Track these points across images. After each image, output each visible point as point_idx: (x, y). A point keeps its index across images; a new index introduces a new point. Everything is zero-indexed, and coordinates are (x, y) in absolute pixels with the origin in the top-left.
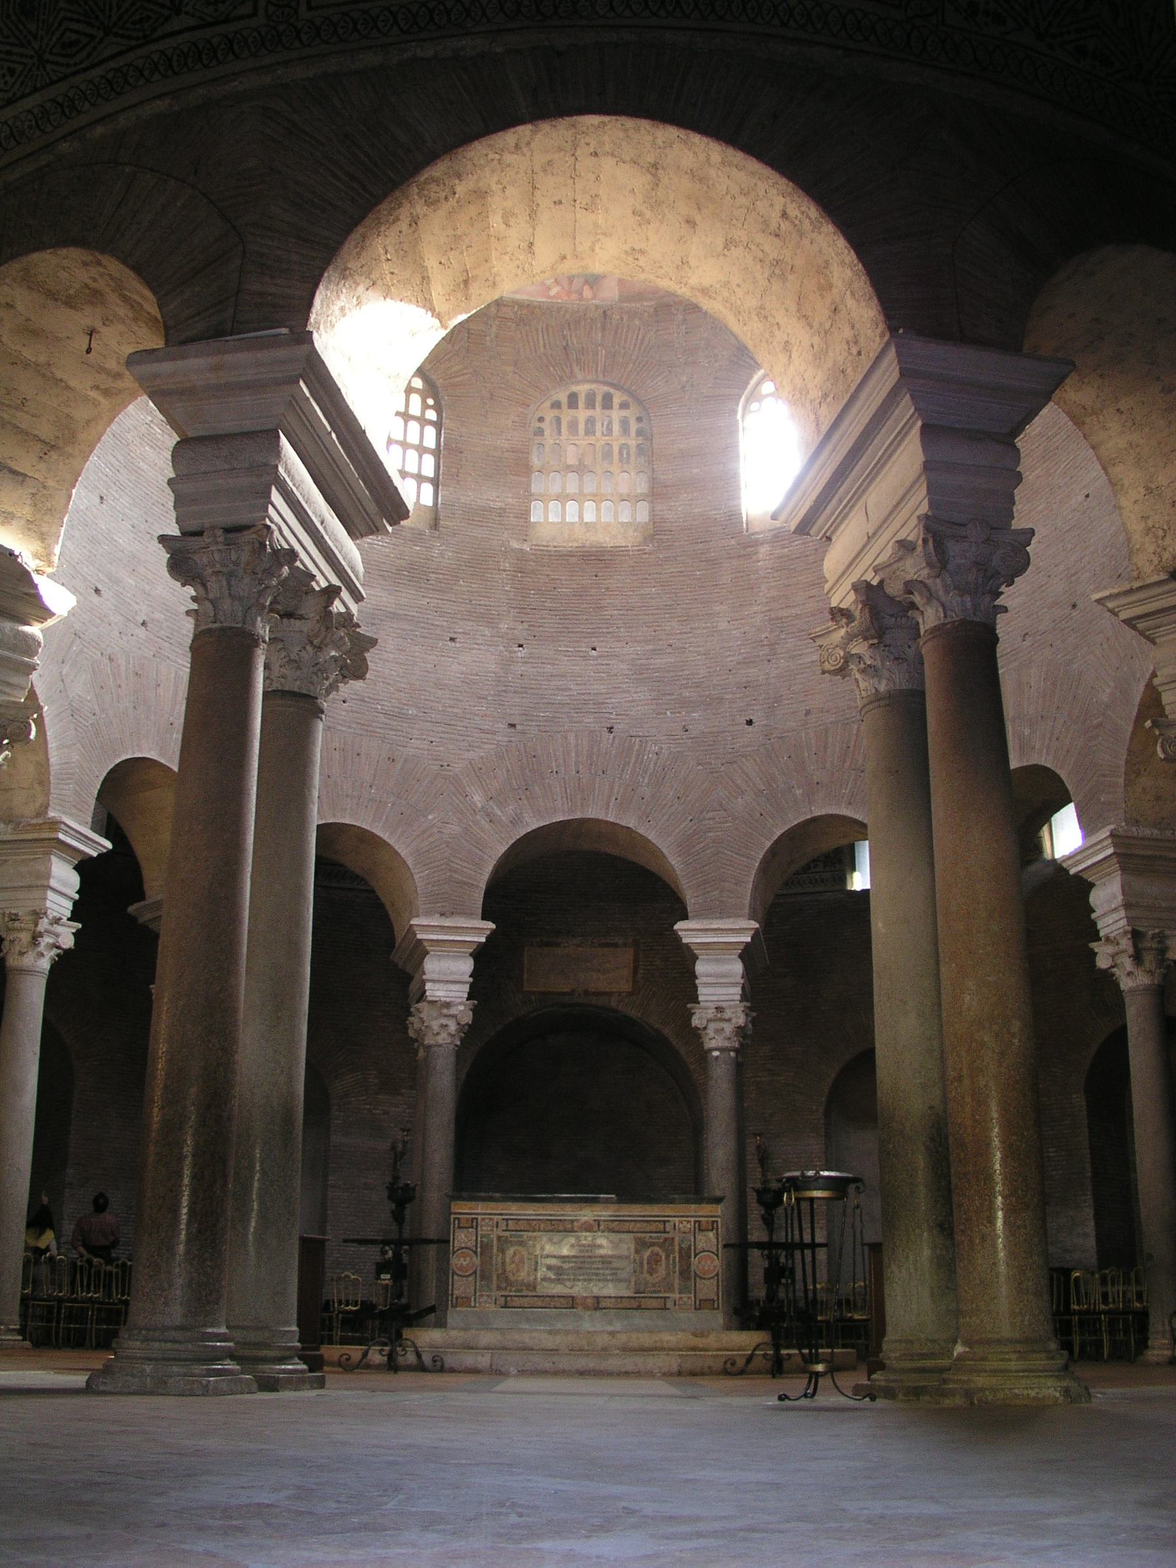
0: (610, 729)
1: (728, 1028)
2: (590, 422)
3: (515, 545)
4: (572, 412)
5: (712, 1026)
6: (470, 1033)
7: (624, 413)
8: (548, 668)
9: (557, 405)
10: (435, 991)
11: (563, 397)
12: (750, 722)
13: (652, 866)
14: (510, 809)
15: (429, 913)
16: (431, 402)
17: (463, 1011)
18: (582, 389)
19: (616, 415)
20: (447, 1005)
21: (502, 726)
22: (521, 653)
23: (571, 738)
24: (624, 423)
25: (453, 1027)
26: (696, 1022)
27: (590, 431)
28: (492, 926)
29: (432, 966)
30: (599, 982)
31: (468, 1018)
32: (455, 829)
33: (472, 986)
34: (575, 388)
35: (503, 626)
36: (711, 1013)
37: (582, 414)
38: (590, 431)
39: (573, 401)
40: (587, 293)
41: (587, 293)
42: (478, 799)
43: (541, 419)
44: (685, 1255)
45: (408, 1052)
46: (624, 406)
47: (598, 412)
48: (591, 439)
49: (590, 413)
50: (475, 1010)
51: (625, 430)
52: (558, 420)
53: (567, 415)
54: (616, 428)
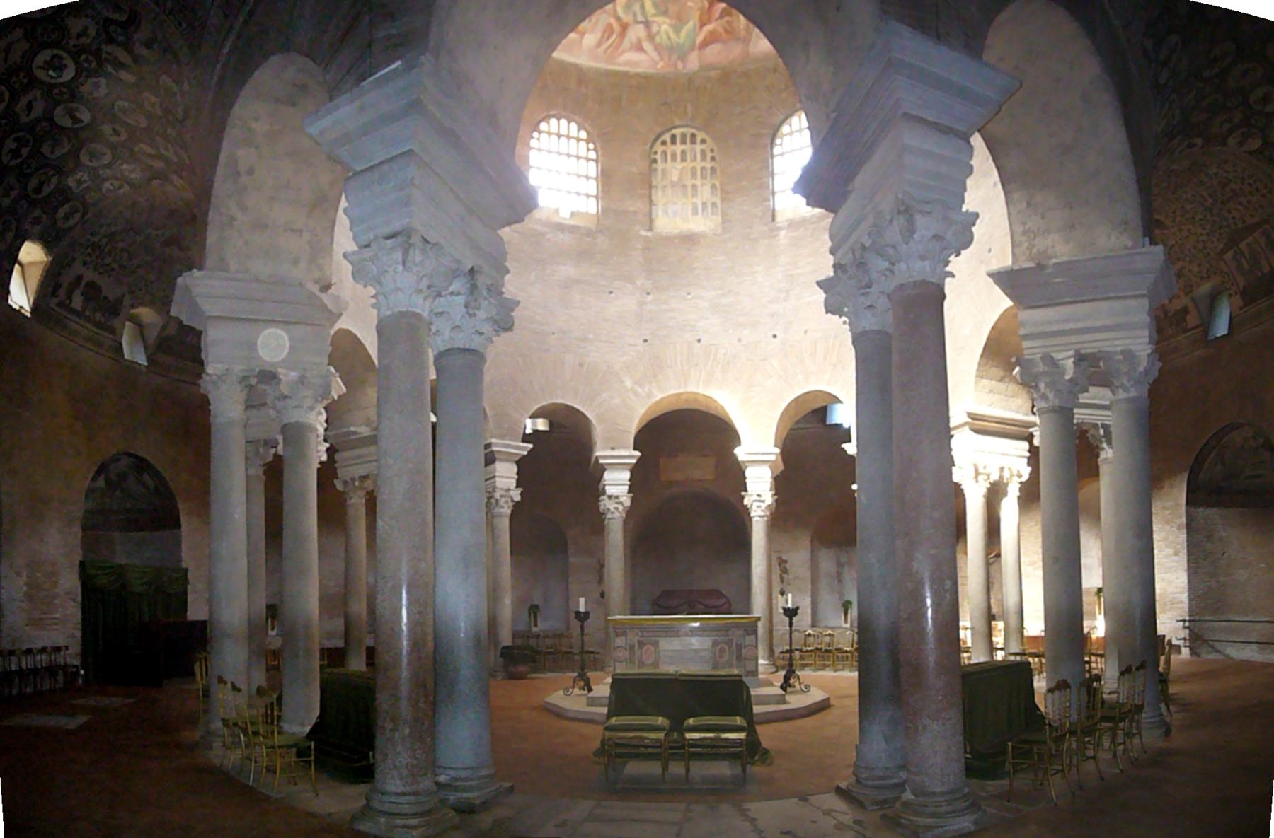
0: (699, 341)
1: (763, 506)
2: (683, 152)
3: (643, 233)
4: (673, 147)
5: (756, 504)
6: (630, 512)
7: (704, 146)
8: (664, 307)
9: (664, 143)
10: (610, 490)
11: (667, 137)
12: (775, 336)
13: (721, 415)
14: (646, 390)
15: (604, 449)
16: (591, 146)
17: (626, 501)
18: (677, 132)
19: (698, 147)
20: (617, 497)
21: (641, 341)
22: (650, 297)
23: (678, 347)
24: (703, 152)
25: (621, 508)
26: (746, 502)
27: (683, 160)
28: (638, 453)
29: (608, 476)
30: (697, 474)
31: (628, 503)
32: (617, 401)
33: (630, 486)
34: (674, 131)
35: (639, 283)
36: (756, 498)
37: (679, 148)
38: (683, 160)
39: (673, 138)
40: (680, 65)
41: (680, 65)
42: (628, 383)
43: (656, 153)
44: (739, 648)
45: (597, 523)
46: (703, 141)
47: (688, 147)
48: (684, 164)
49: (683, 147)
50: (633, 500)
51: (704, 158)
52: (665, 153)
53: (670, 149)
54: (699, 156)
